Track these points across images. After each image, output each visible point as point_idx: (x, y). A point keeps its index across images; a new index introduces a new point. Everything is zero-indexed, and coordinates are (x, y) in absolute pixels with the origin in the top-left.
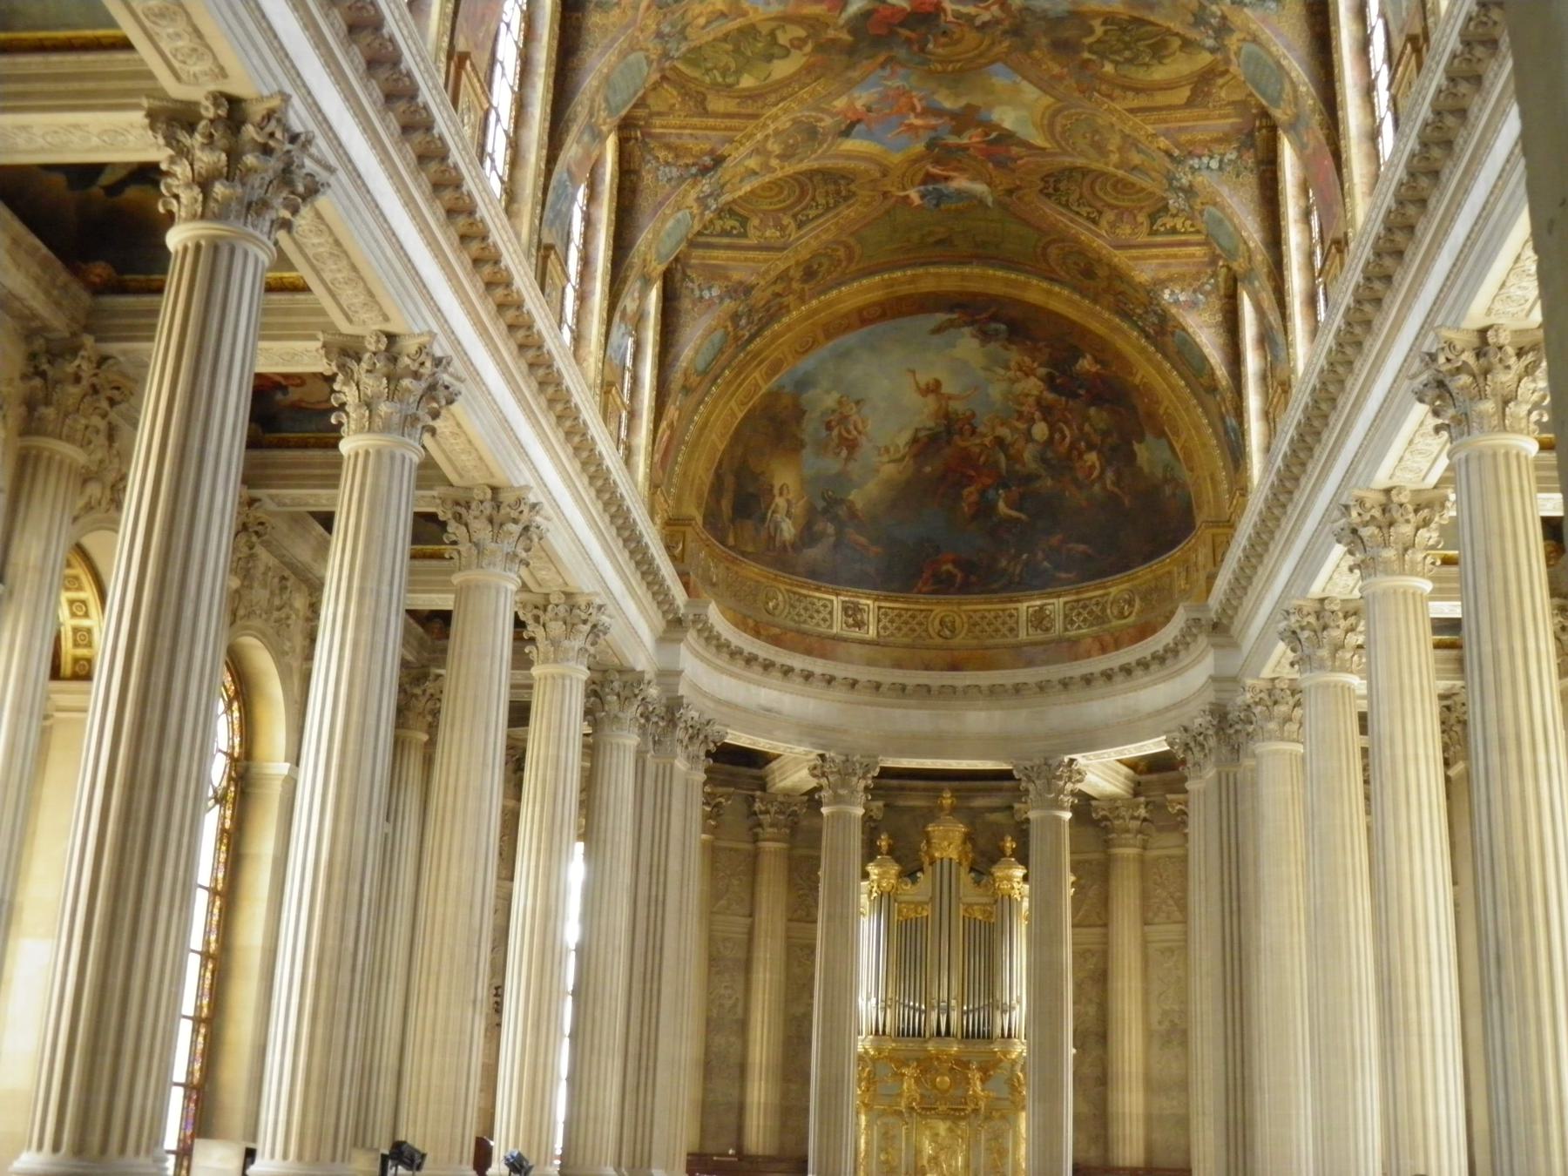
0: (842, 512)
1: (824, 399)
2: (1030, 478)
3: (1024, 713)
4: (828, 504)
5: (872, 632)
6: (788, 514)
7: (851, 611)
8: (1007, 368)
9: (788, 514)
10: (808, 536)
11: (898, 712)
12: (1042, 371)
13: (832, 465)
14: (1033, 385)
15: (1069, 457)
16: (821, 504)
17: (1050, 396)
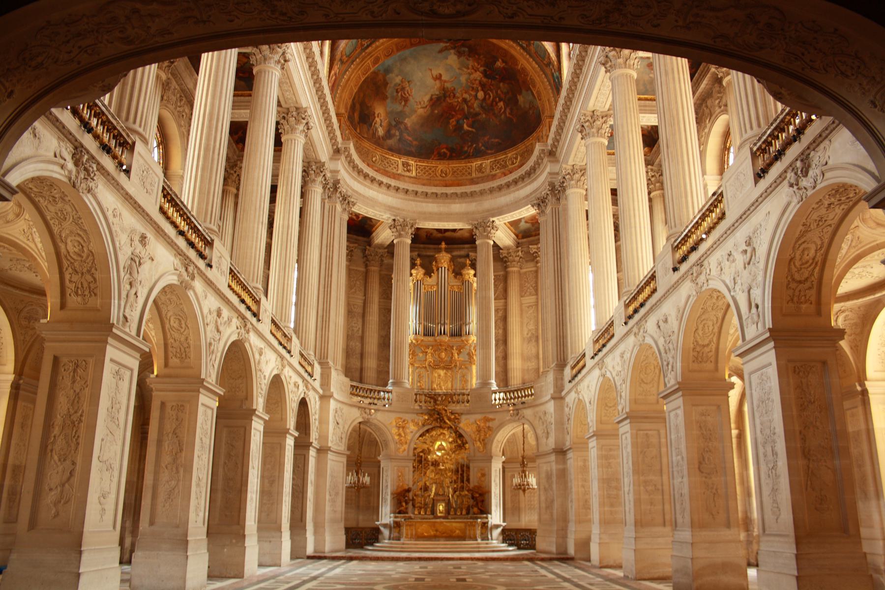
0: (402, 127)
1: (395, 79)
2: (477, 114)
3: (474, 204)
4: (396, 122)
5: (414, 174)
6: (381, 125)
7: (406, 165)
8: (468, 68)
9: (381, 125)
10: (388, 135)
11: (424, 204)
12: (482, 69)
13: (398, 108)
14: (478, 75)
15: (492, 105)
16: (394, 123)
17: (484, 80)
